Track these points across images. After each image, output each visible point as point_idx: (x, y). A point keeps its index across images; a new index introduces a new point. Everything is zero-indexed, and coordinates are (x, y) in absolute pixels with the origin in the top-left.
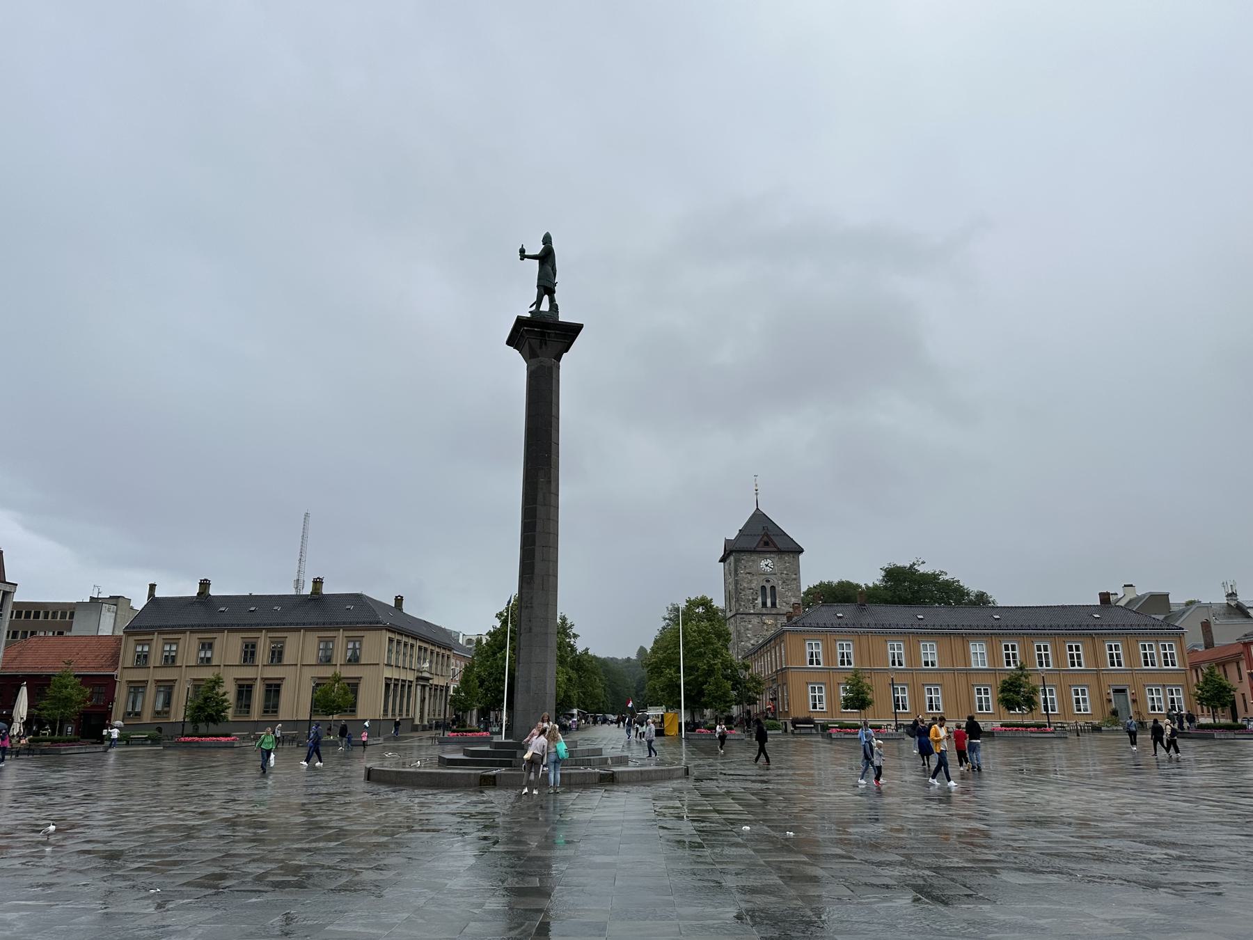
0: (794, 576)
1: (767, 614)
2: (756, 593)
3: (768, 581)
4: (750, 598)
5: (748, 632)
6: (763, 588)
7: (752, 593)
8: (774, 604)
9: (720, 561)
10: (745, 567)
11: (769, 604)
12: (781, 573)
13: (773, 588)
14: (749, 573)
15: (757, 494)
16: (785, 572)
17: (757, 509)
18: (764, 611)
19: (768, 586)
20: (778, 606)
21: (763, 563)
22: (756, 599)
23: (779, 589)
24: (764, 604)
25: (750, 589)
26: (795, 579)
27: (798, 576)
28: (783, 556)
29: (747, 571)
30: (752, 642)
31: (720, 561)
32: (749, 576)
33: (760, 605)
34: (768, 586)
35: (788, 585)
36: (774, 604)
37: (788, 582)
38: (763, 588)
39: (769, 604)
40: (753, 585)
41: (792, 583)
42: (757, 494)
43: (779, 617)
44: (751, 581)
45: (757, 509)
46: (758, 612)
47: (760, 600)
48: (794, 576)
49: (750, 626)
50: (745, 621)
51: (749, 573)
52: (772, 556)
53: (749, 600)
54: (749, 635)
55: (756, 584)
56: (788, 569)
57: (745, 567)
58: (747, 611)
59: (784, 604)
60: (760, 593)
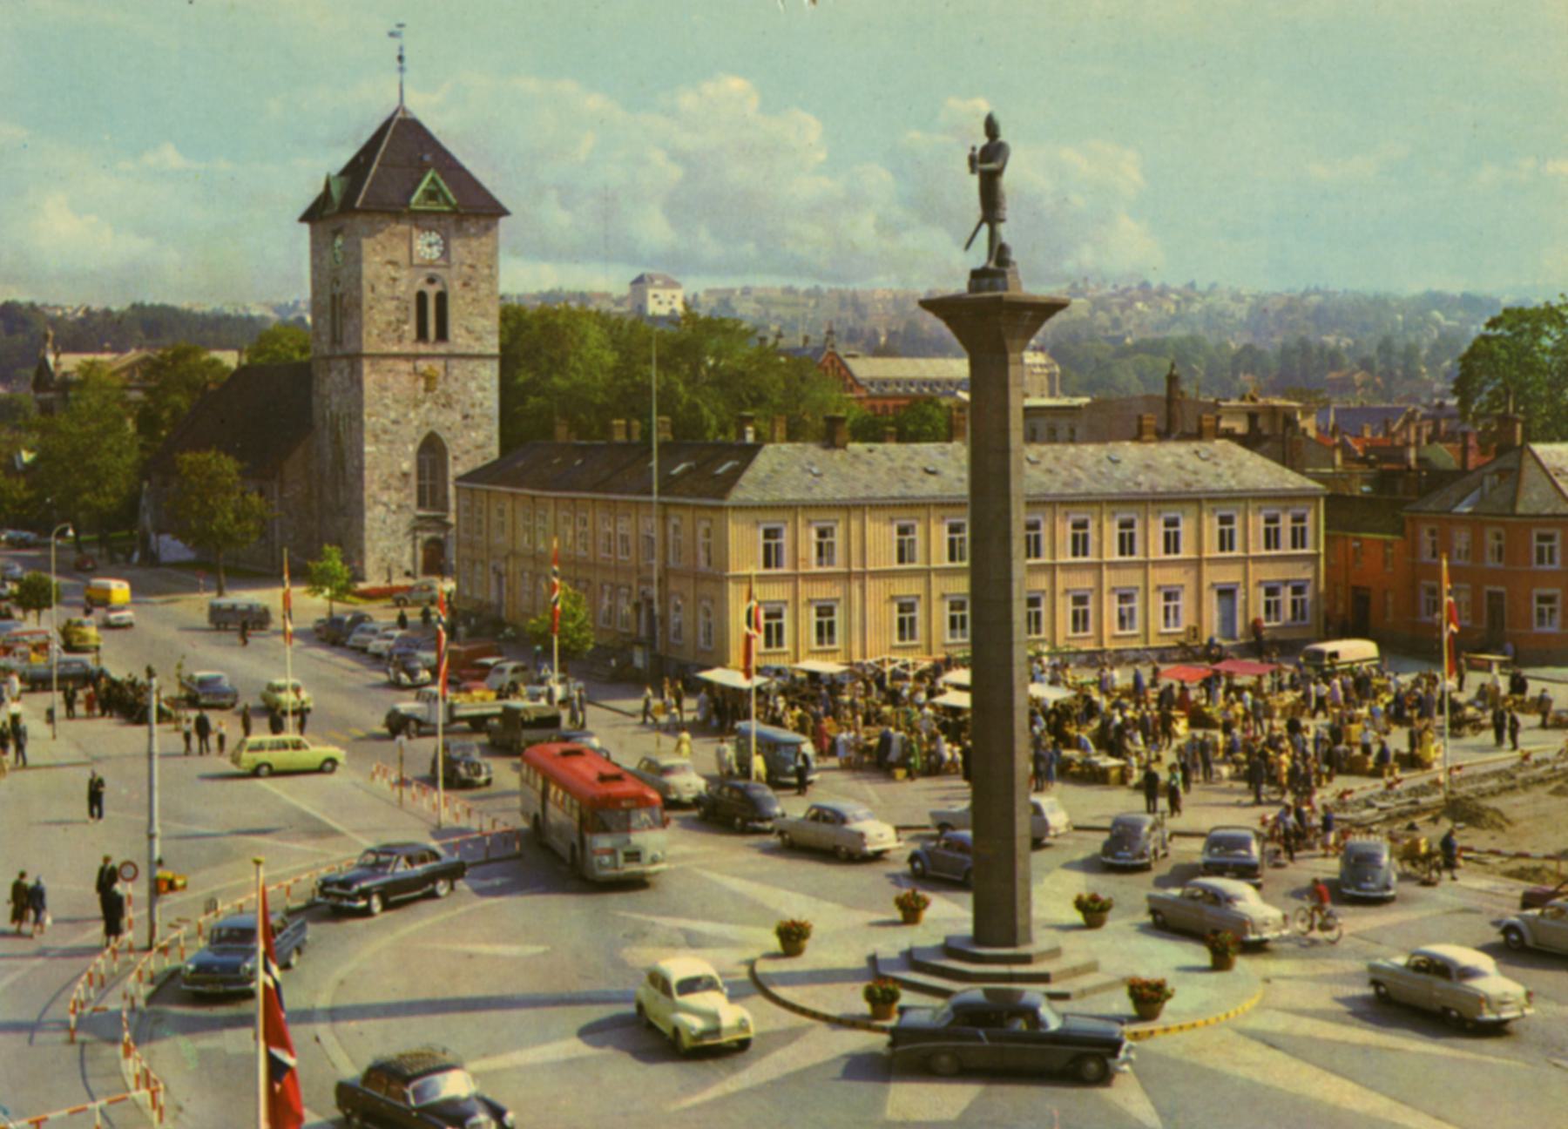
3: (431, 281)
6: (421, 297)
9: (304, 219)
13: (442, 298)
16: (469, 261)
18: (423, 348)
24: (422, 335)
28: (465, 224)
29: (388, 257)
30: (393, 415)
31: (304, 219)
34: (432, 291)
36: (442, 335)
43: (453, 362)
47: (410, 328)
54: (387, 401)
55: (409, 284)
60: (413, 308)
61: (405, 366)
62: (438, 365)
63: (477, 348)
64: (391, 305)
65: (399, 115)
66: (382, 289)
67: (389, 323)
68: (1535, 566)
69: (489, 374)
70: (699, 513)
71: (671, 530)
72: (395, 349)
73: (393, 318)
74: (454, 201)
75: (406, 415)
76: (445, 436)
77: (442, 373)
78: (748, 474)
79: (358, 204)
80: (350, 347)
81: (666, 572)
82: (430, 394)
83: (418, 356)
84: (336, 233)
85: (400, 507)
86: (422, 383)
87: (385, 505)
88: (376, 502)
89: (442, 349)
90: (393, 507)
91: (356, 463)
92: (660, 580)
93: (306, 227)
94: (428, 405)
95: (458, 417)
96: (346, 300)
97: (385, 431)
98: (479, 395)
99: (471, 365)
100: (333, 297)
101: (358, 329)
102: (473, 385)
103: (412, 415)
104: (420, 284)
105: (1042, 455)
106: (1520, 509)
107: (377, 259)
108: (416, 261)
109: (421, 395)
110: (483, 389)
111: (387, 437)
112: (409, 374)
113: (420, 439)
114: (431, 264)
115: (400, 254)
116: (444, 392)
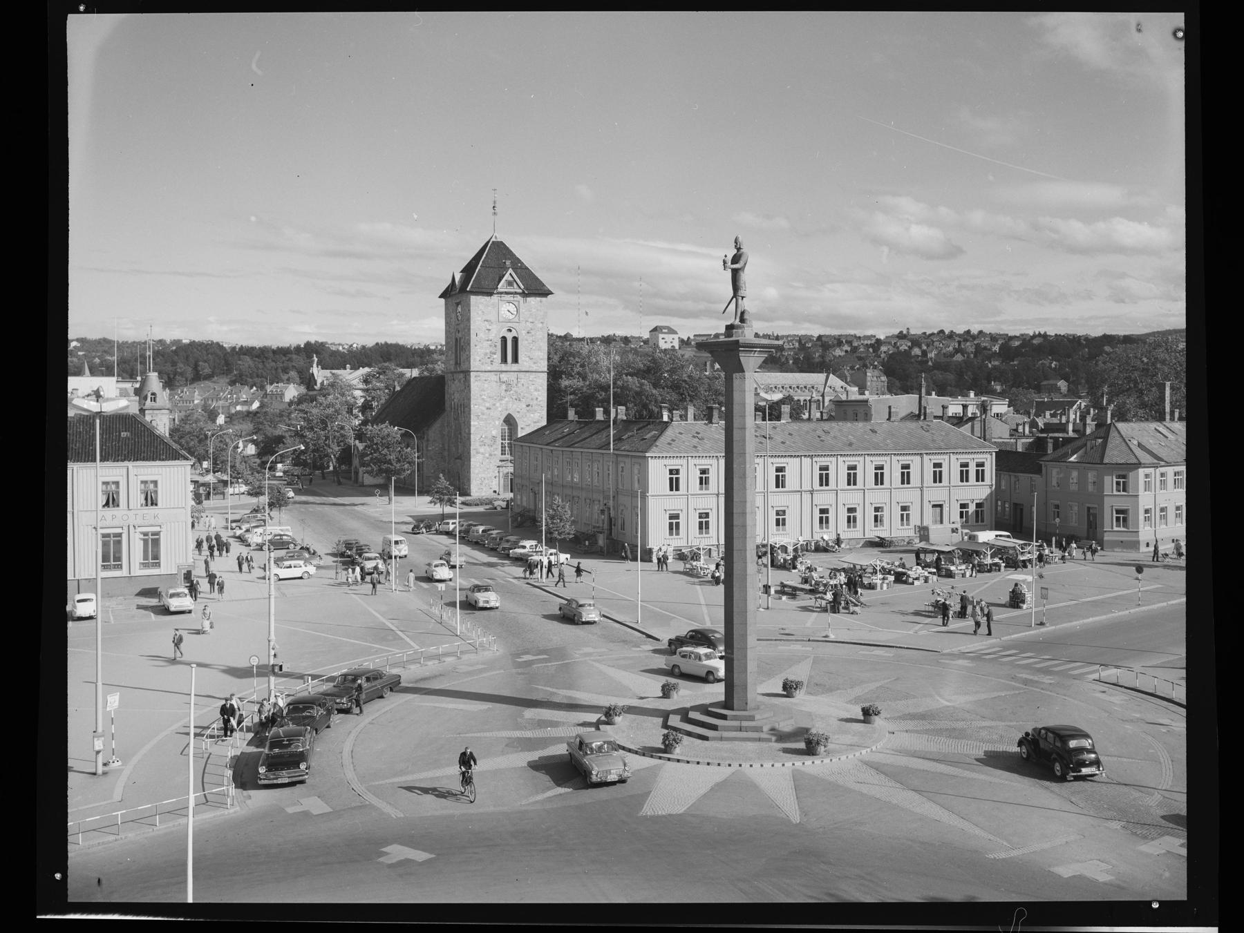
3: (510, 330)
6: (504, 339)
9: (440, 297)
10: (483, 312)
12: (527, 321)
13: (515, 340)
14: (487, 321)
16: (530, 320)
18: (504, 367)
19: (509, 337)
24: (504, 360)
28: (528, 299)
30: (487, 405)
31: (440, 297)
34: (509, 337)
35: (532, 335)
36: (515, 360)
47: (498, 356)
51: (487, 321)
54: (483, 397)
55: (497, 332)
57: (483, 312)
61: (493, 377)
62: (513, 376)
63: (535, 368)
64: (486, 344)
65: (493, 239)
66: (481, 335)
67: (486, 354)
68: (1115, 493)
69: (542, 382)
70: (633, 460)
71: (620, 469)
72: (489, 368)
73: (488, 351)
74: (522, 287)
75: (494, 405)
76: (516, 416)
77: (515, 381)
78: (662, 439)
79: (468, 289)
80: (464, 367)
81: (617, 492)
82: (508, 393)
84: (458, 304)
85: (490, 455)
86: (504, 387)
87: (482, 454)
88: (478, 453)
89: (515, 367)
90: (487, 455)
91: (467, 431)
92: (614, 497)
93: (443, 300)
94: (507, 399)
95: (524, 406)
96: (462, 340)
97: (483, 414)
98: (536, 393)
99: (532, 376)
100: (457, 339)
101: (469, 357)
102: (532, 388)
103: (498, 405)
104: (504, 333)
105: (832, 428)
106: (1106, 460)
107: (480, 319)
108: (501, 319)
109: (503, 393)
110: (536, 390)
111: (484, 417)
112: (496, 382)
113: (503, 418)
114: (510, 321)
115: (493, 317)
116: (516, 392)
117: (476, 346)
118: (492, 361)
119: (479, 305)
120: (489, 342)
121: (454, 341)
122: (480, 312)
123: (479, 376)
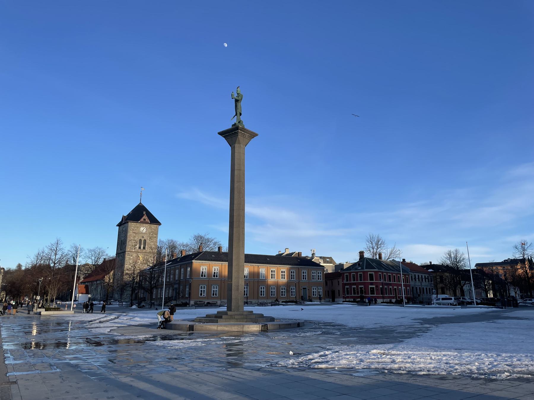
0: (155, 236)
1: (140, 252)
2: (137, 242)
4: (134, 244)
5: (130, 260)
6: (140, 240)
7: (135, 242)
8: (144, 248)
9: (117, 226)
11: (142, 248)
13: (145, 241)
15: (141, 196)
16: (151, 234)
17: (140, 203)
19: (143, 240)
20: (146, 249)
21: (142, 229)
22: (136, 245)
23: (147, 241)
24: (140, 248)
25: (134, 240)
26: (155, 237)
27: (157, 235)
29: (134, 232)
31: (117, 226)
32: (134, 234)
33: (138, 248)
34: (143, 240)
36: (144, 248)
37: (152, 238)
38: (140, 240)
39: (142, 248)
40: (136, 239)
41: (154, 239)
42: (141, 196)
44: (135, 236)
45: (140, 203)
46: (136, 251)
47: (138, 246)
48: (155, 236)
49: (132, 257)
50: (129, 255)
51: (134, 233)
52: (147, 225)
53: (133, 245)
54: (130, 262)
56: (153, 232)
58: (131, 250)
59: (149, 248)
60: (138, 242)
72: (134, 251)
73: (134, 244)
83: (138, 252)
117: (129, 242)
118: (135, 248)
119: (132, 225)
120: (135, 241)
121: (121, 241)
122: (132, 230)
123: (129, 254)
